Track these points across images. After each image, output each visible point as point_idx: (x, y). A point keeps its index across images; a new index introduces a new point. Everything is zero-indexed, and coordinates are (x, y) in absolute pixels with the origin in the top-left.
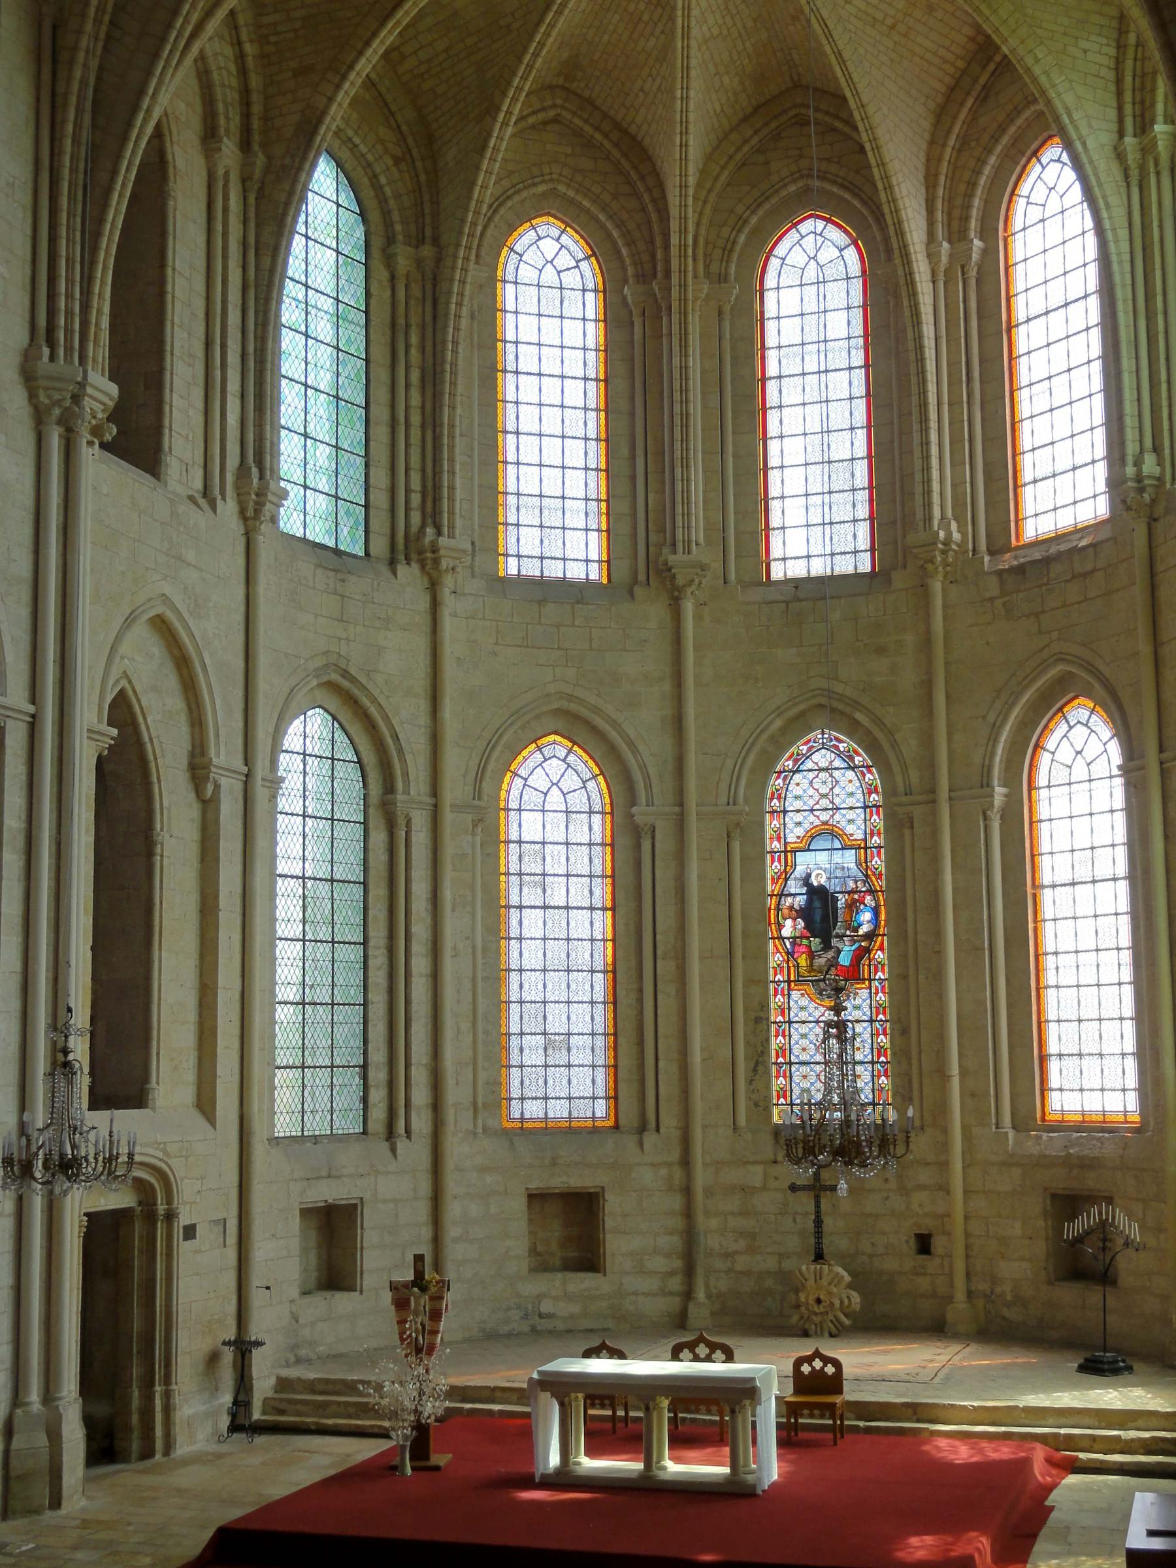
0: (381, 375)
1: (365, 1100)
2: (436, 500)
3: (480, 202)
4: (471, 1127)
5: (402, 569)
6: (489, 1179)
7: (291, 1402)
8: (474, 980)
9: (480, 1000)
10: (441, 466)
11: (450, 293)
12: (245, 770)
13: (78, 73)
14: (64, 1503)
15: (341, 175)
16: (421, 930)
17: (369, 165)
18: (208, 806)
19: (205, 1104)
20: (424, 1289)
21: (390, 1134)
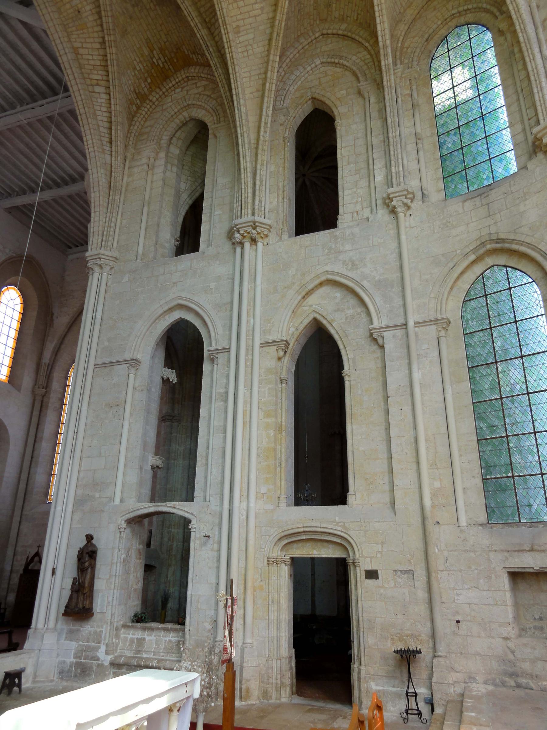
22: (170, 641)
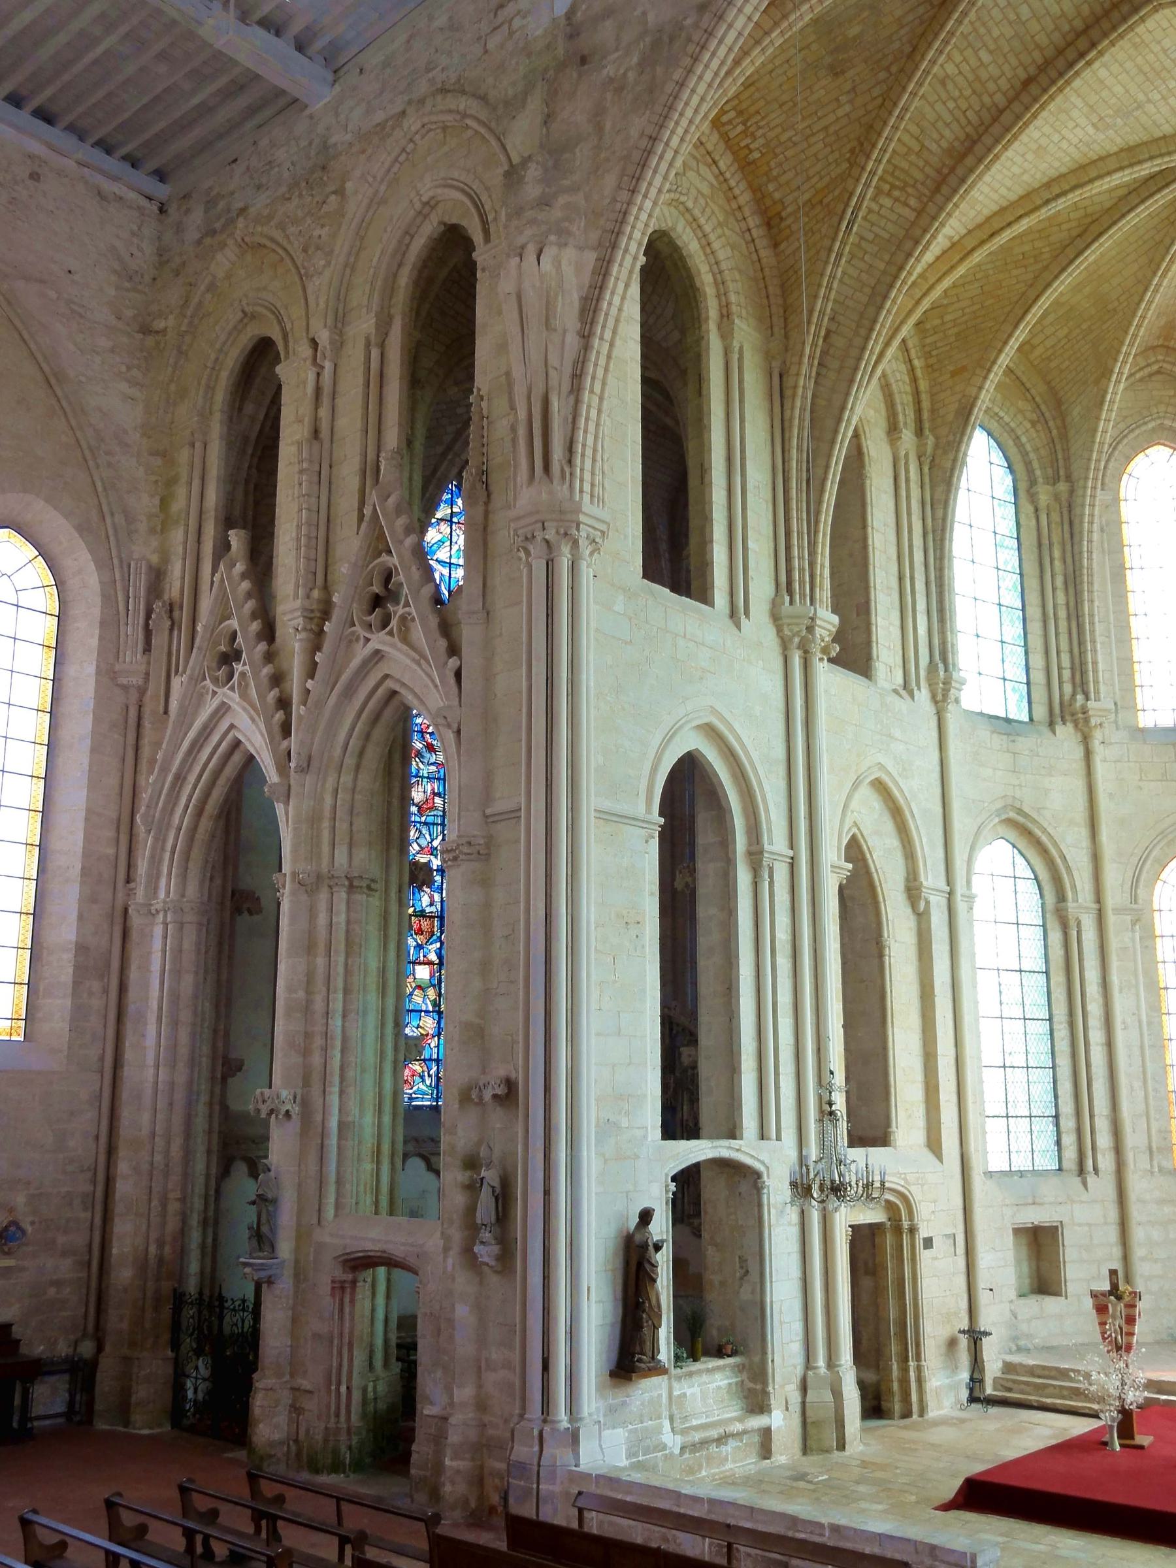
0: (1033, 583)
1: (1058, 1143)
2: (1083, 673)
3: (1102, 444)
4: (1148, 1167)
5: (1059, 728)
6: (1167, 1210)
7: (1014, 1381)
8: (1142, 1047)
9: (1148, 1064)
10: (1086, 647)
11: (1082, 515)
12: (948, 889)
13: (798, 403)
14: (847, 1447)
15: (992, 441)
16: (1095, 1008)
17: (1013, 430)
18: (922, 918)
19: (934, 1144)
20: (1119, 1298)
21: (1081, 1171)
22: (719, 1388)
